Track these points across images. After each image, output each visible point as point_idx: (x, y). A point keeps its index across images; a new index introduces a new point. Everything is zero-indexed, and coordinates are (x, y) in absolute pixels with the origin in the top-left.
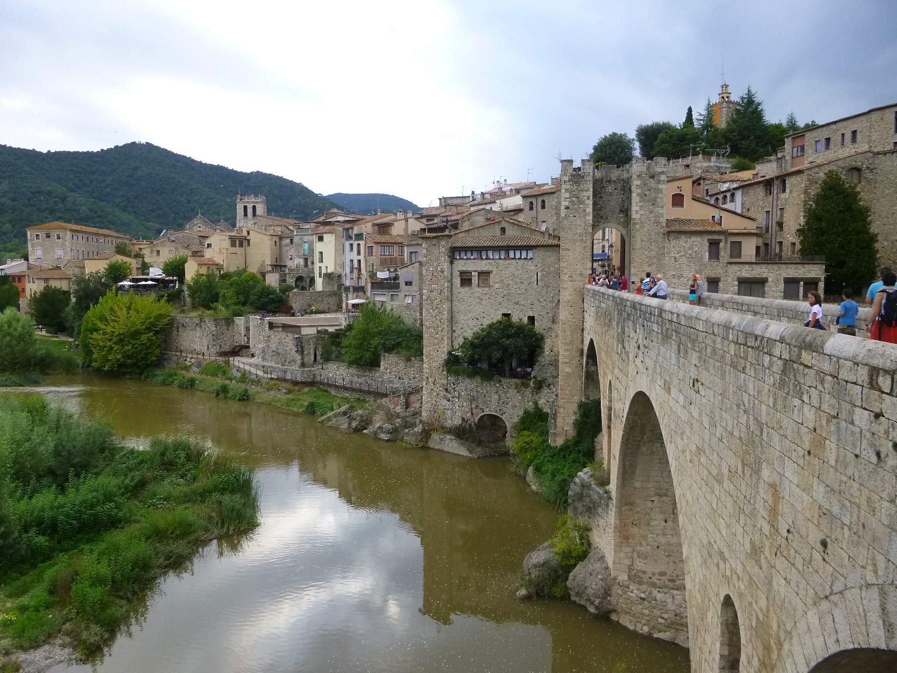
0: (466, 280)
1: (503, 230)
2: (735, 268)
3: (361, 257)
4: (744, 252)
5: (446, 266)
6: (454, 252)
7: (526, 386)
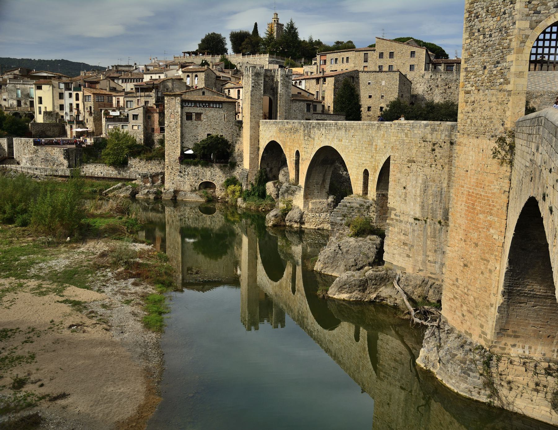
0: (189, 116)
1: (204, 93)
2: (316, 115)
3: (80, 102)
4: (317, 109)
5: (179, 110)
6: (184, 102)
7: (225, 166)
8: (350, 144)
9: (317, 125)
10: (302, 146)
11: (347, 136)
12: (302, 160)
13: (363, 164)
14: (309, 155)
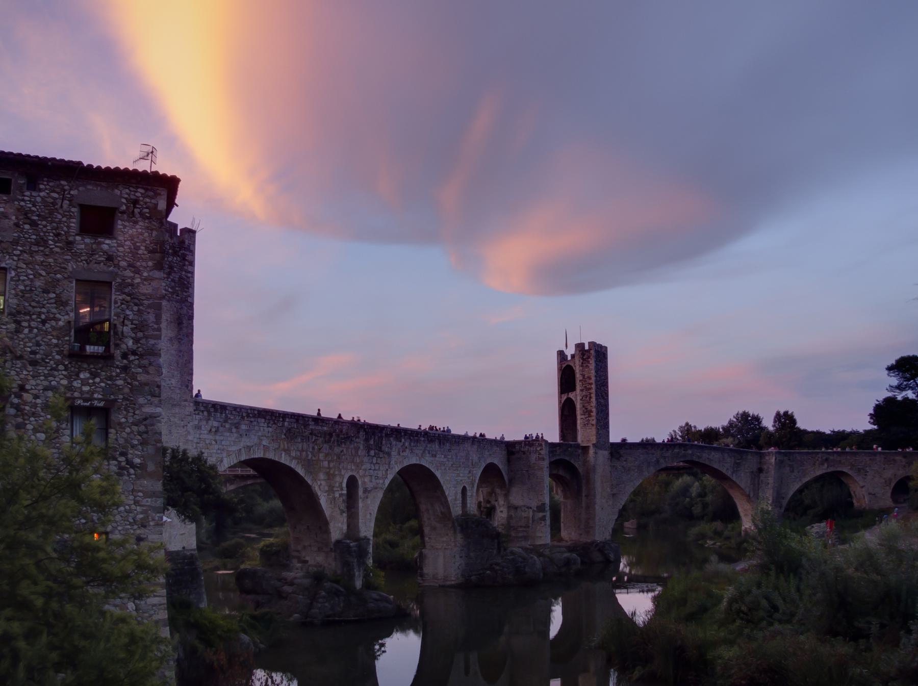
8: (445, 460)
9: (395, 433)
10: (363, 467)
11: (442, 450)
12: (366, 491)
13: (461, 480)
14: (381, 481)
